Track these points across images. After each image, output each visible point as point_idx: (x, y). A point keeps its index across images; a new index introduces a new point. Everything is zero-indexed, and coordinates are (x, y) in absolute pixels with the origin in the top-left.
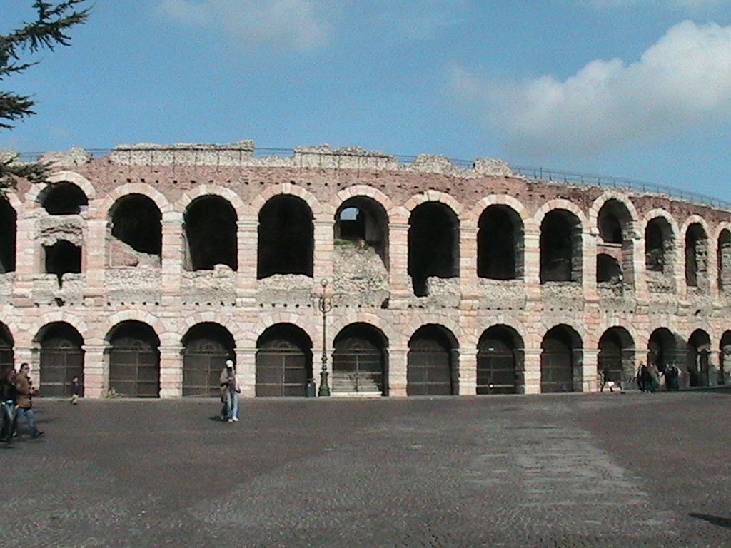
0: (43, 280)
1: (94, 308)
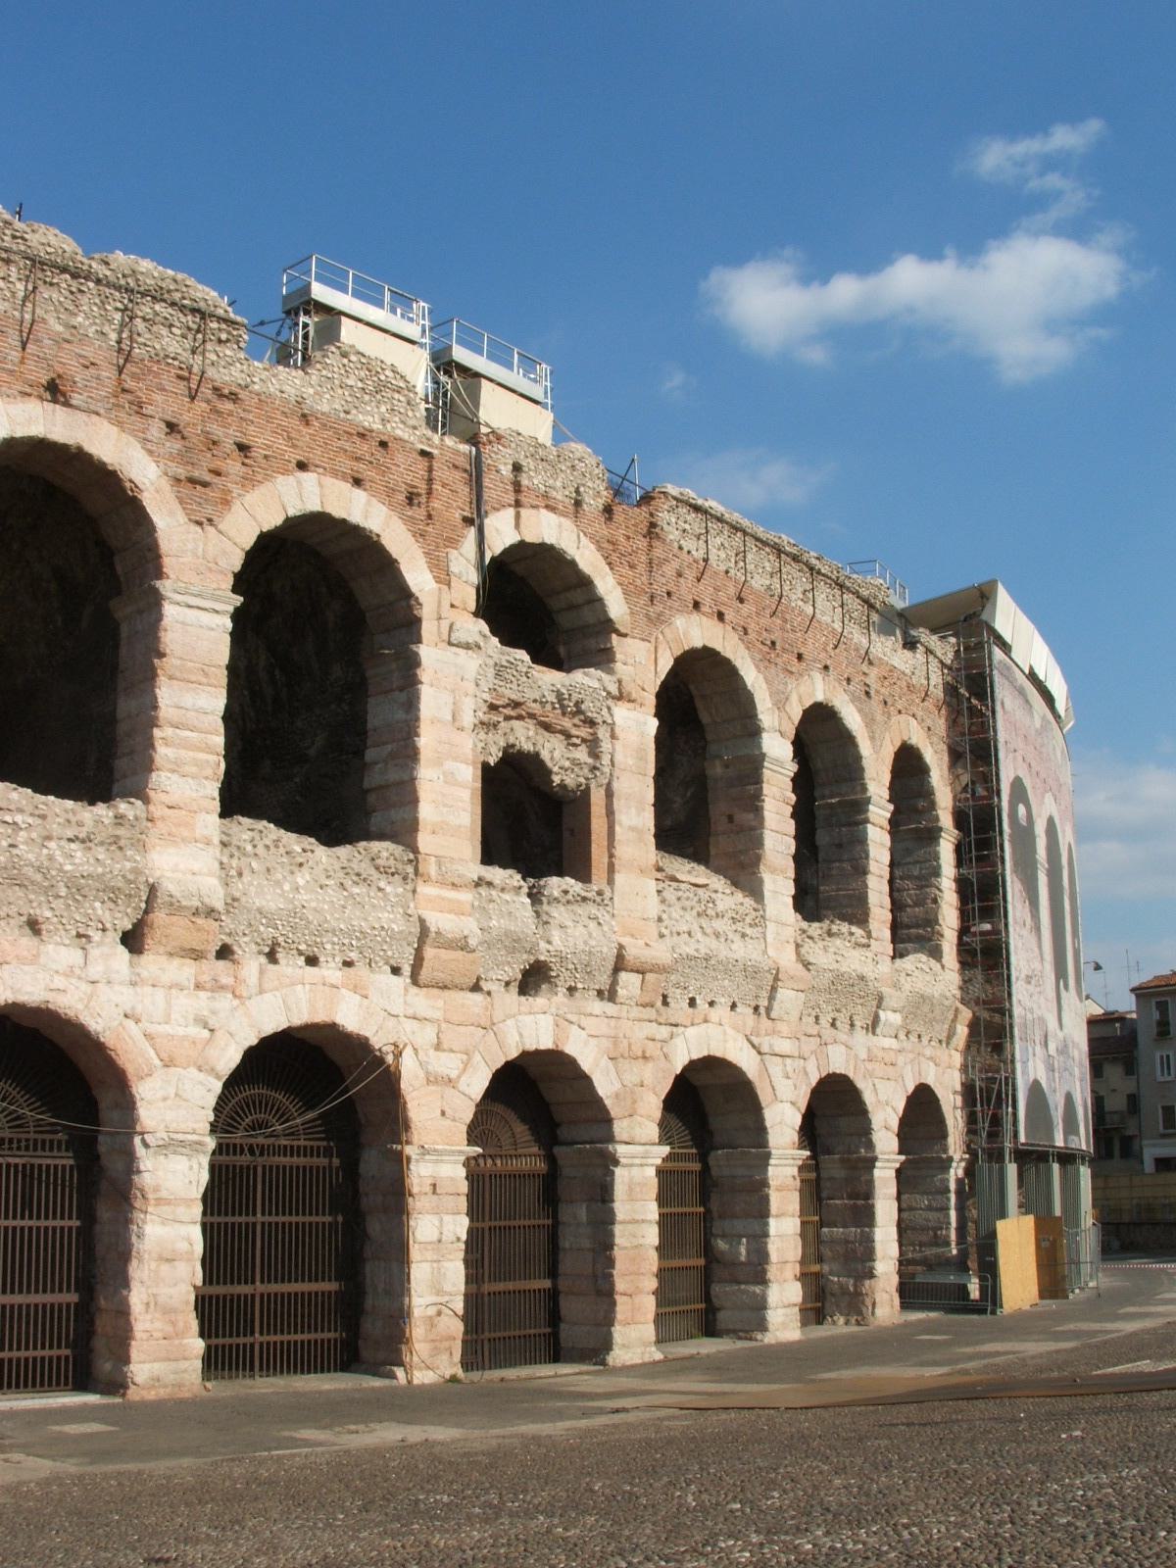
0: (503, 890)
1: (636, 1012)
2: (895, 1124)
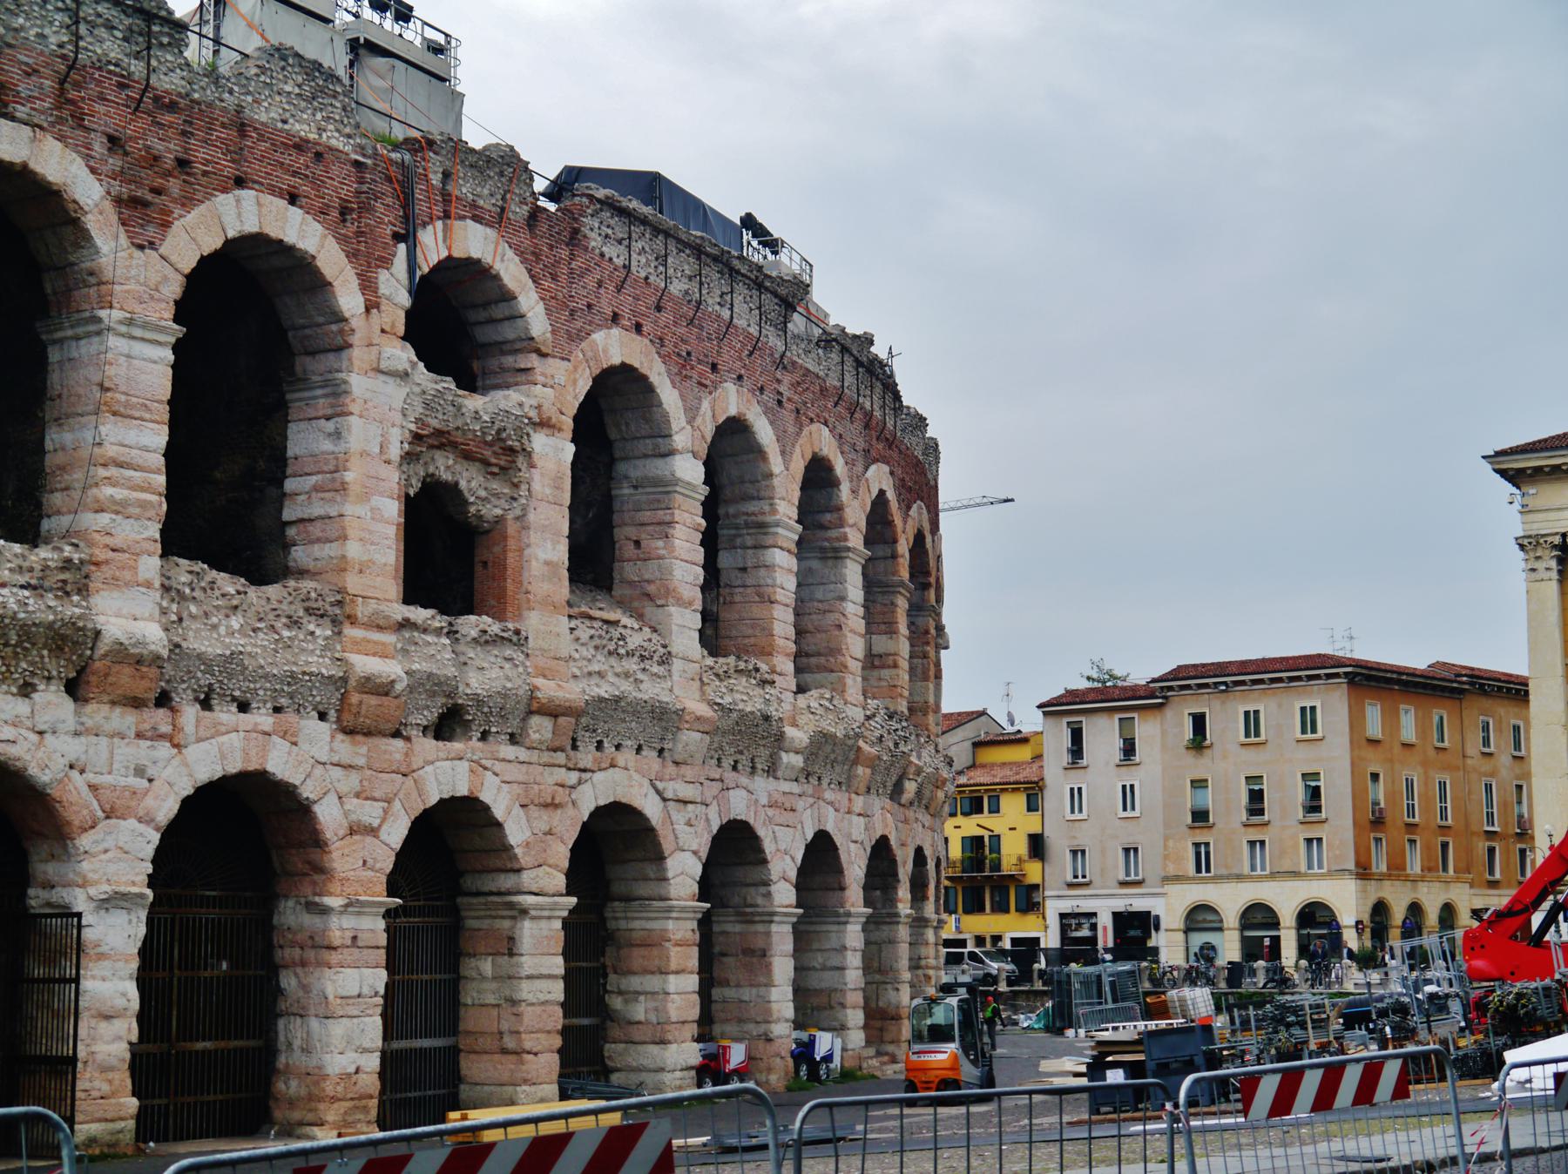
0: (425, 631)
1: (547, 757)
2: (793, 874)
